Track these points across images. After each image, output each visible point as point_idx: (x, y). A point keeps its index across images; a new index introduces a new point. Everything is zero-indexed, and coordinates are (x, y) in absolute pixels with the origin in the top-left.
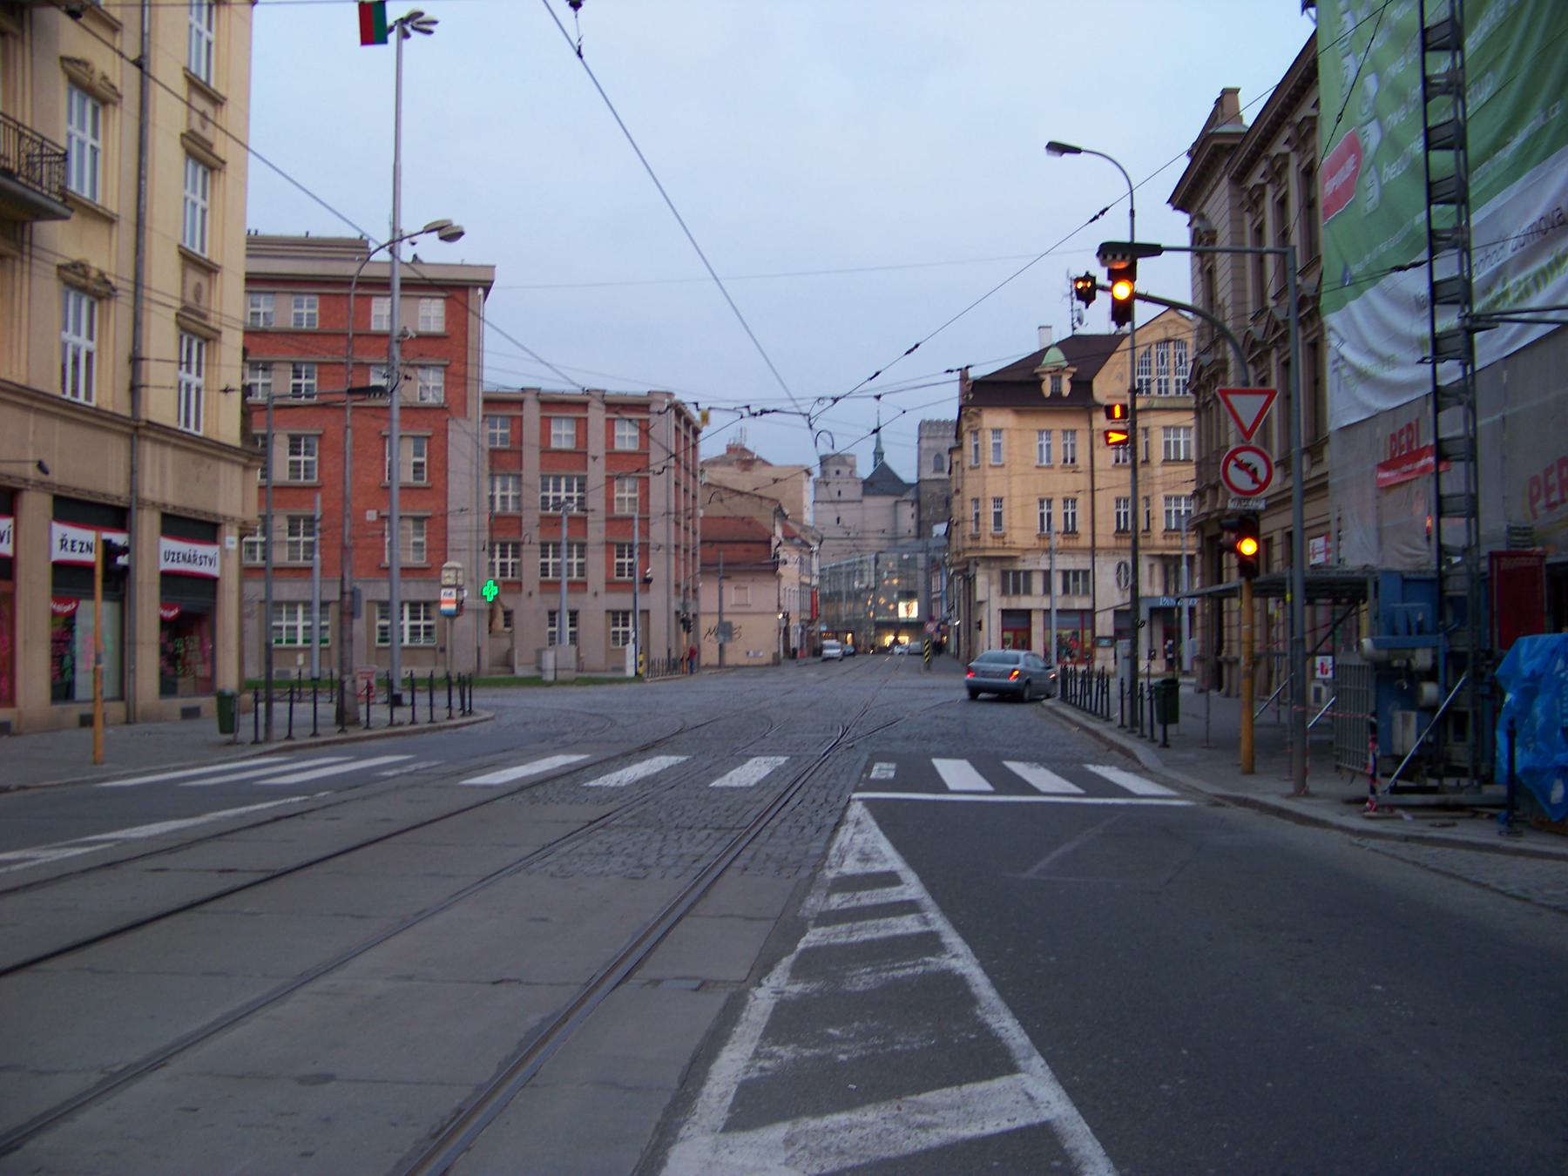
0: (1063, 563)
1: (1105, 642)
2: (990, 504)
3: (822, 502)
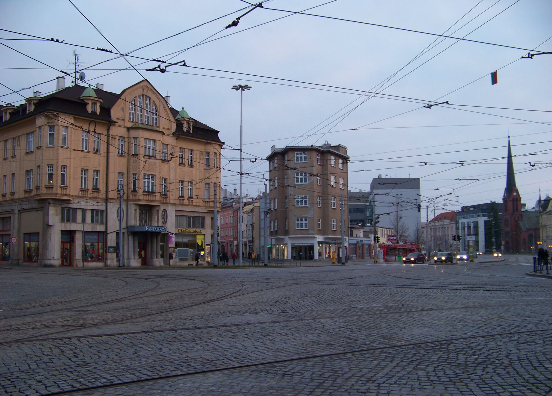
0: (90, 206)
1: (111, 250)
2: (60, 169)
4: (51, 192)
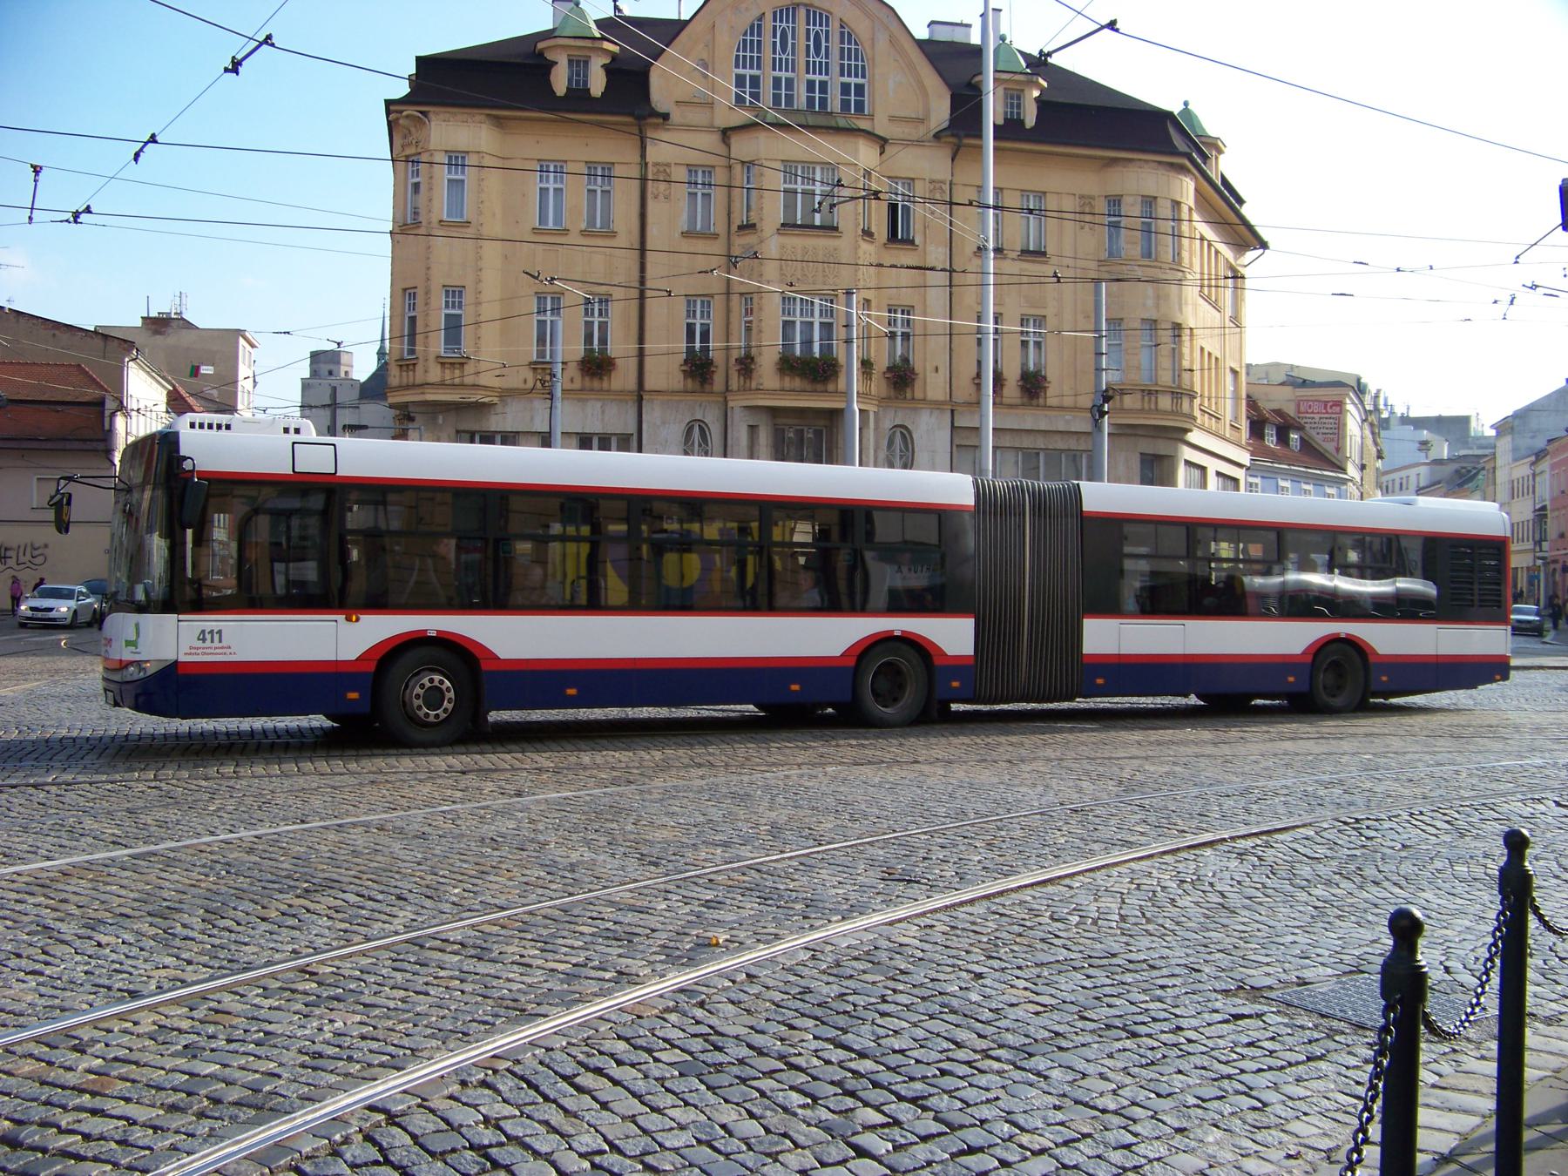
2: (438, 299)
3: (311, 407)
4: (457, 381)
